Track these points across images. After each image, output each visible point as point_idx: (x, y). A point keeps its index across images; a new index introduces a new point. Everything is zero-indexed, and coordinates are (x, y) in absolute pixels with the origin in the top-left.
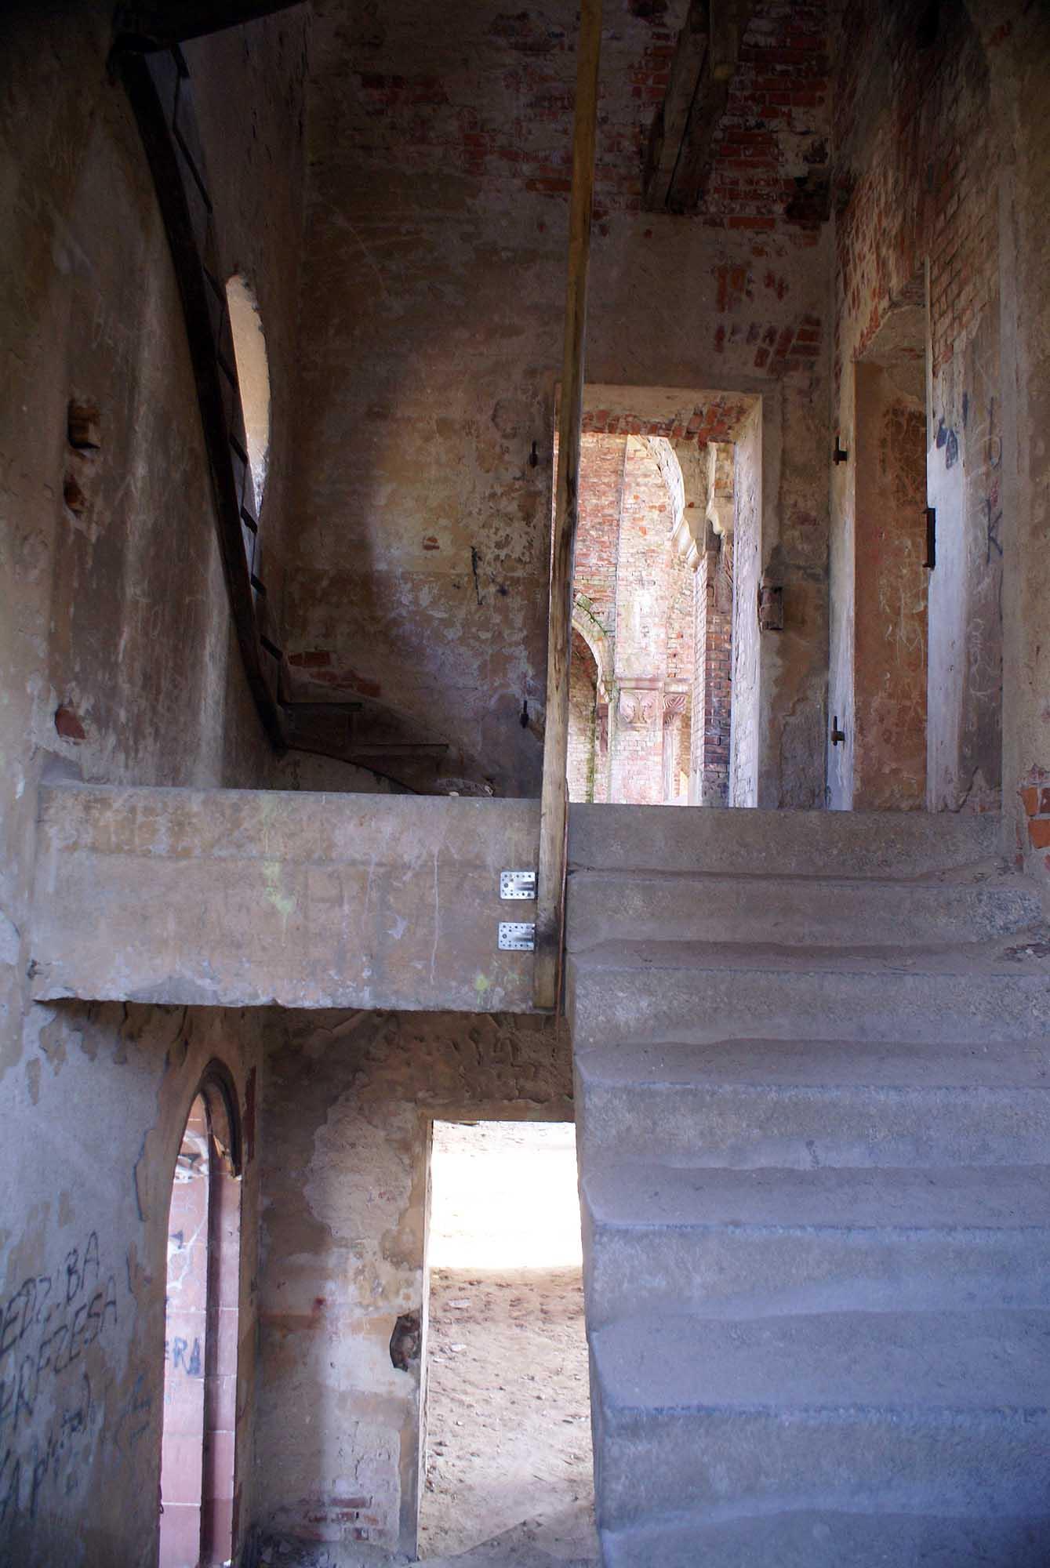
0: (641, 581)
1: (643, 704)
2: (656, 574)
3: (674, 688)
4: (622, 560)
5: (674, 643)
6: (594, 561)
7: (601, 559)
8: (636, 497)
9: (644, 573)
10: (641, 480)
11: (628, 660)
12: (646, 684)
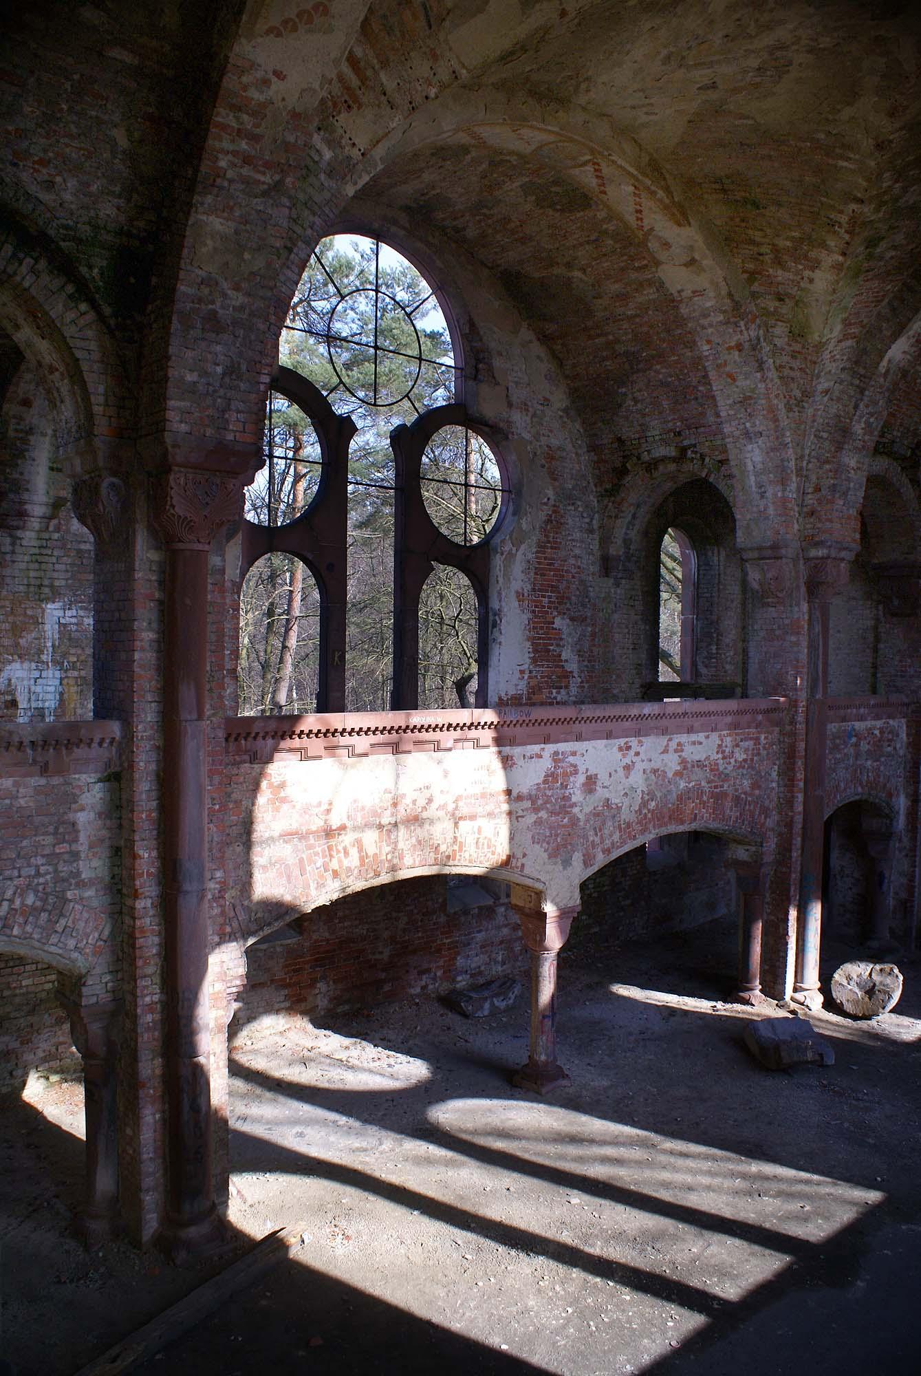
0: (747, 434)
1: (769, 575)
2: (760, 423)
3: (813, 553)
4: (723, 414)
5: (810, 500)
8: (709, 342)
9: (748, 425)
10: (705, 322)
11: (748, 527)
12: (769, 553)
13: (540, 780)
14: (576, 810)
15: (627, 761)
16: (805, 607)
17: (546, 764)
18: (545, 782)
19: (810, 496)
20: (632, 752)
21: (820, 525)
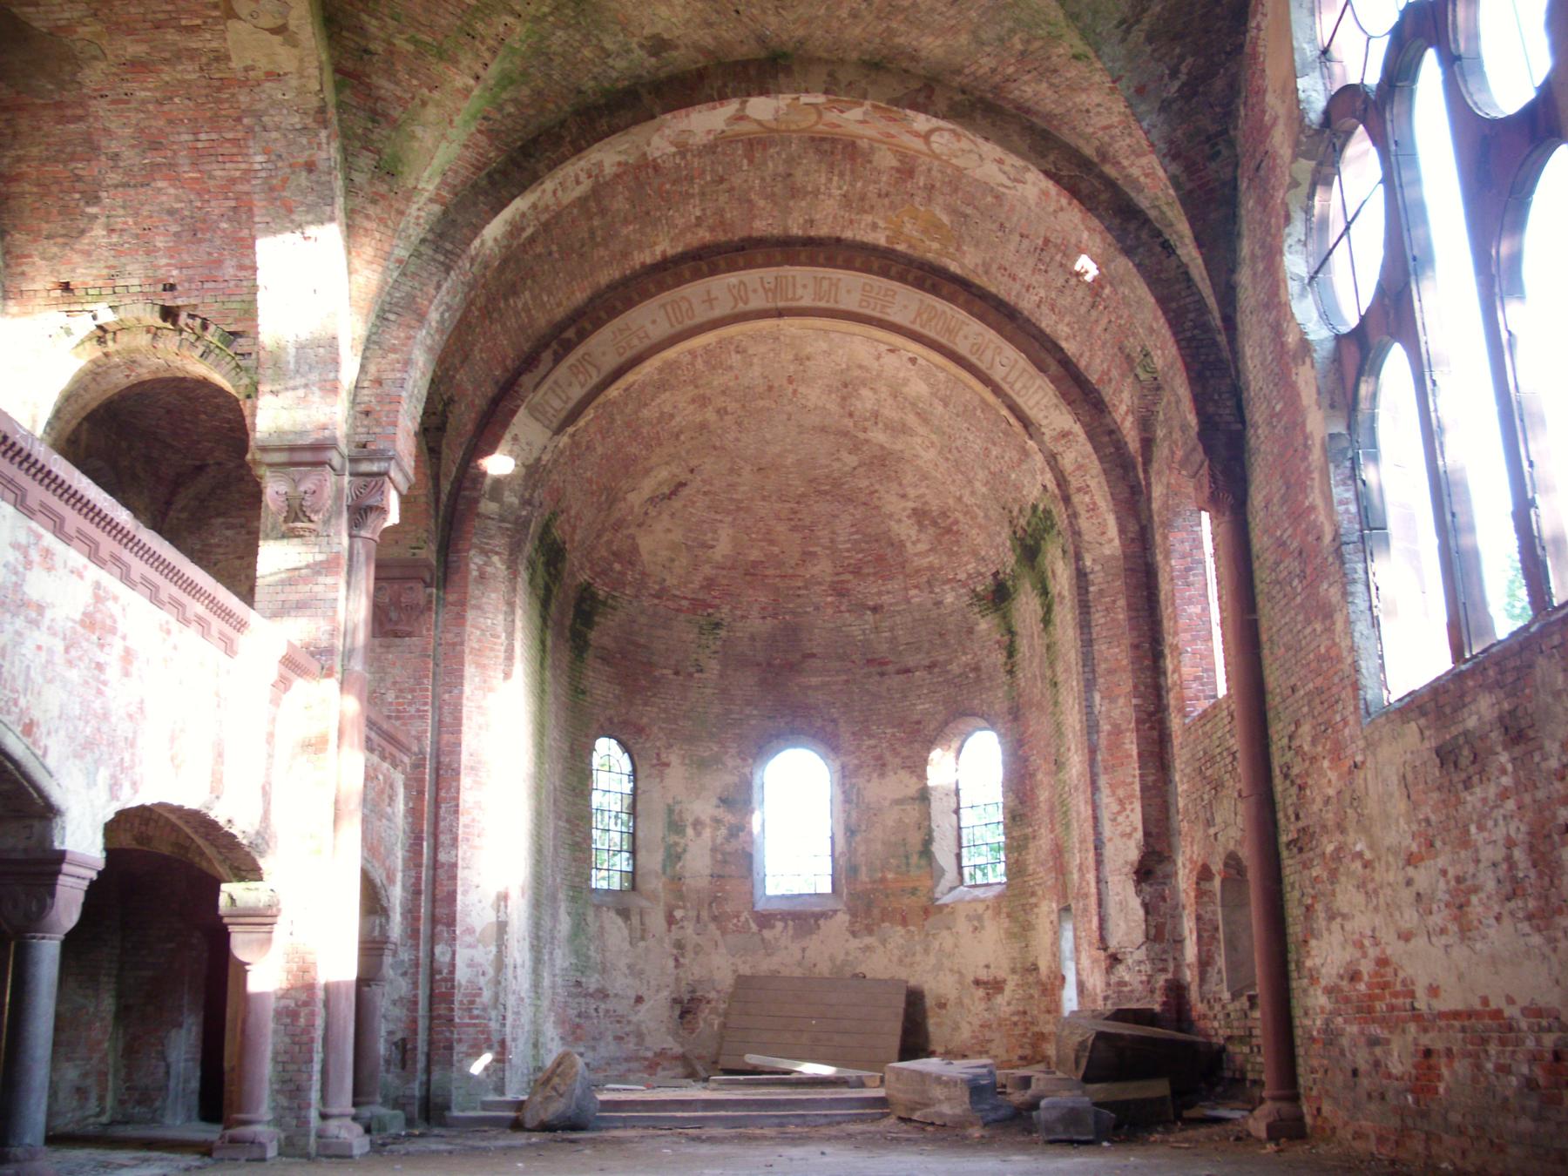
3: (365, 467)
6: (231, 271)
7: (241, 267)
12: (307, 456)
13: (78, 617)
16: (345, 540)
18: (82, 623)
19: (365, 392)
21: (378, 430)
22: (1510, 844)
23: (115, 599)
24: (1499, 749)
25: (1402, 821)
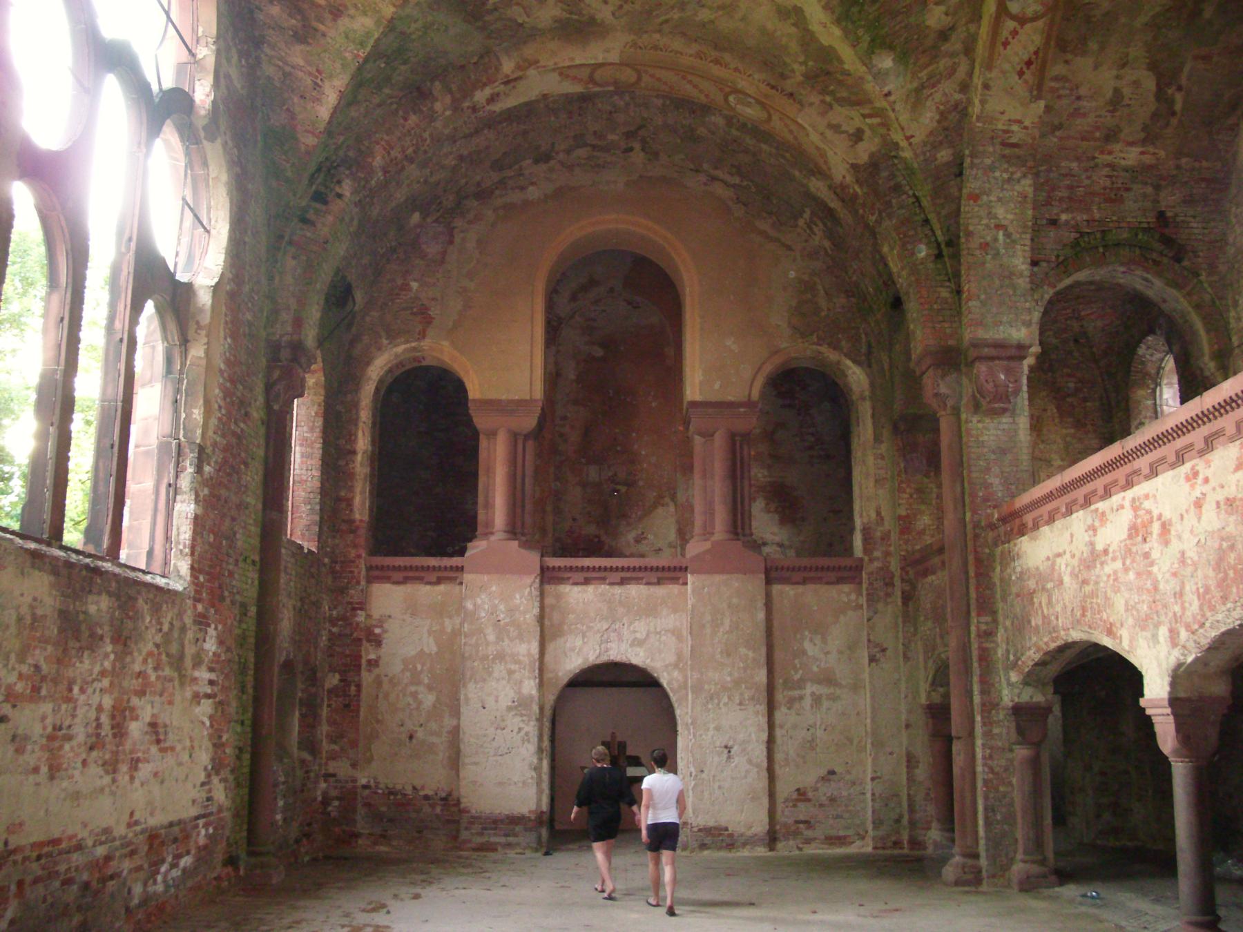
14: (1155, 569)
15: (1197, 493)
17: (1126, 516)
18: (1130, 537)
20: (1201, 477)
22: (100, 709)
23: (1147, 497)
24: (108, 640)
25: (13, 657)
